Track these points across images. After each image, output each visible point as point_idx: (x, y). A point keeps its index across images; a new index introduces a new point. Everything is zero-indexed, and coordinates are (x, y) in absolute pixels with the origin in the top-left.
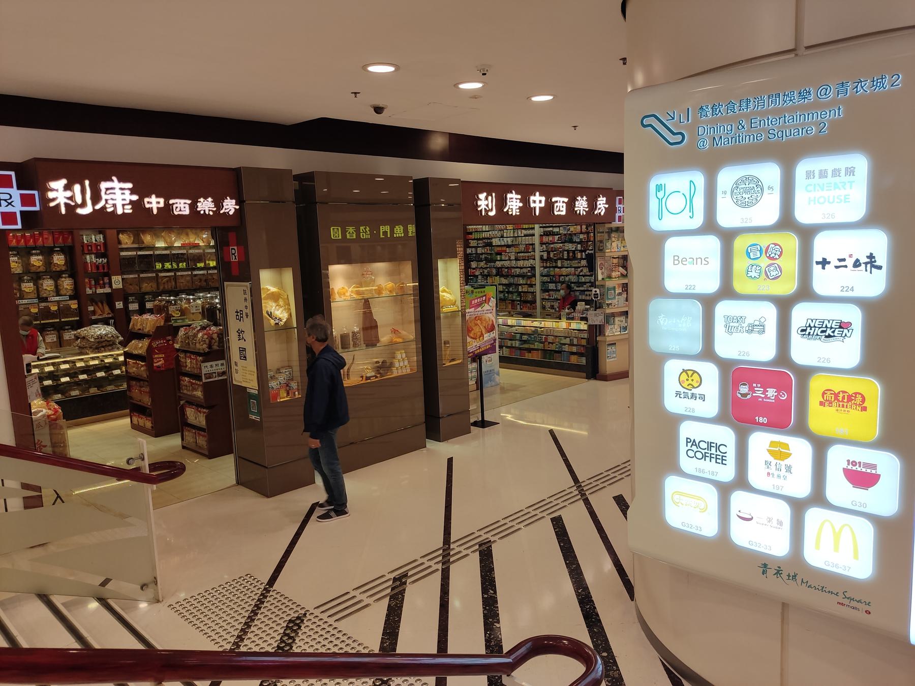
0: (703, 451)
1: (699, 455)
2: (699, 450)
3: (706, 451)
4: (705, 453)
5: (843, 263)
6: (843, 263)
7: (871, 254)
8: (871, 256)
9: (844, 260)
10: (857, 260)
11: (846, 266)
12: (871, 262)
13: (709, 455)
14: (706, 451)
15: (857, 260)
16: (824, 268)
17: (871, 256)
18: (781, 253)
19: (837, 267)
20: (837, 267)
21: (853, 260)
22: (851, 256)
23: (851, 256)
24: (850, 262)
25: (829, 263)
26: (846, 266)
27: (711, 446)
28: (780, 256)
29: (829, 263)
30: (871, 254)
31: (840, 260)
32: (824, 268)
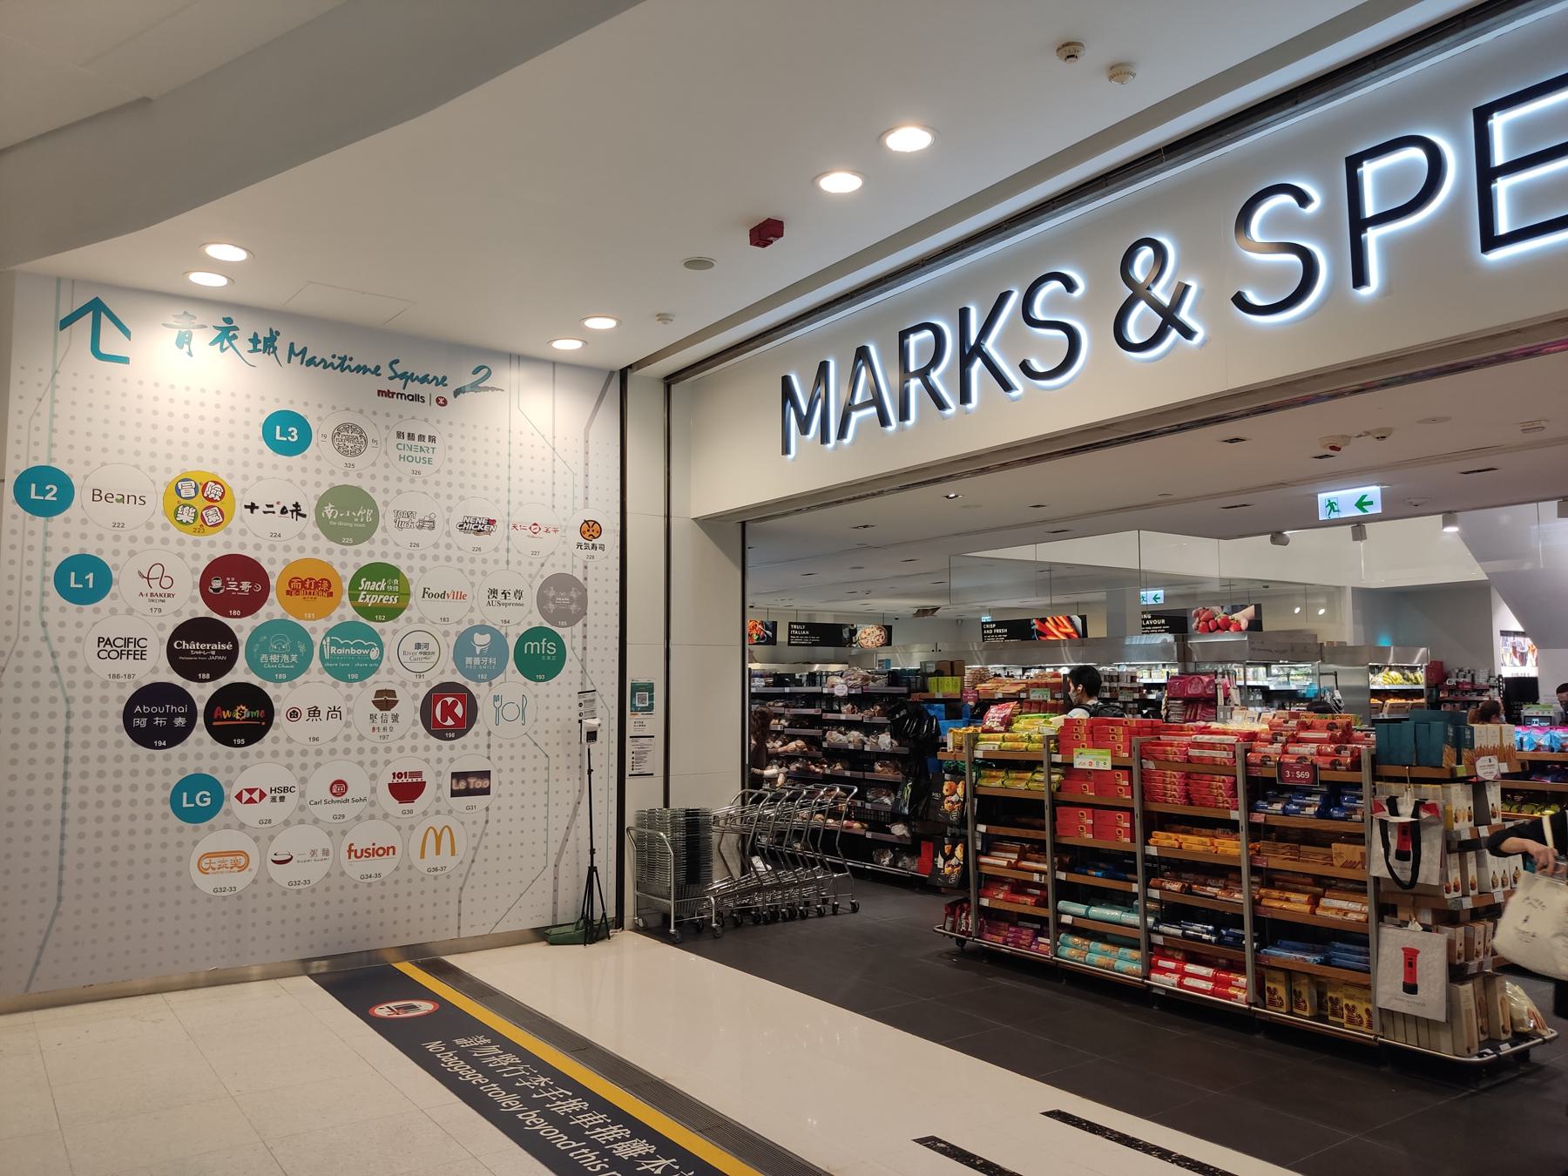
0: (119, 650)
1: (113, 654)
2: (114, 648)
3: (123, 648)
4: (121, 651)
5: (270, 509)
6: (270, 509)
7: (297, 503)
8: (296, 505)
9: (272, 506)
10: (284, 508)
11: (274, 512)
12: (297, 511)
13: (126, 652)
14: (123, 648)
15: (284, 508)
16: (252, 512)
17: (296, 505)
18: (223, 493)
19: (265, 512)
20: (265, 512)
21: (281, 507)
22: (278, 503)
23: (278, 503)
24: (277, 509)
25: (257, 508)
26: (274, 512)
27: (128, 642)
28: (221, 498)
29: (257, 508)
30: (297, 503)
31: (268, 506)
32: (252, 512)
